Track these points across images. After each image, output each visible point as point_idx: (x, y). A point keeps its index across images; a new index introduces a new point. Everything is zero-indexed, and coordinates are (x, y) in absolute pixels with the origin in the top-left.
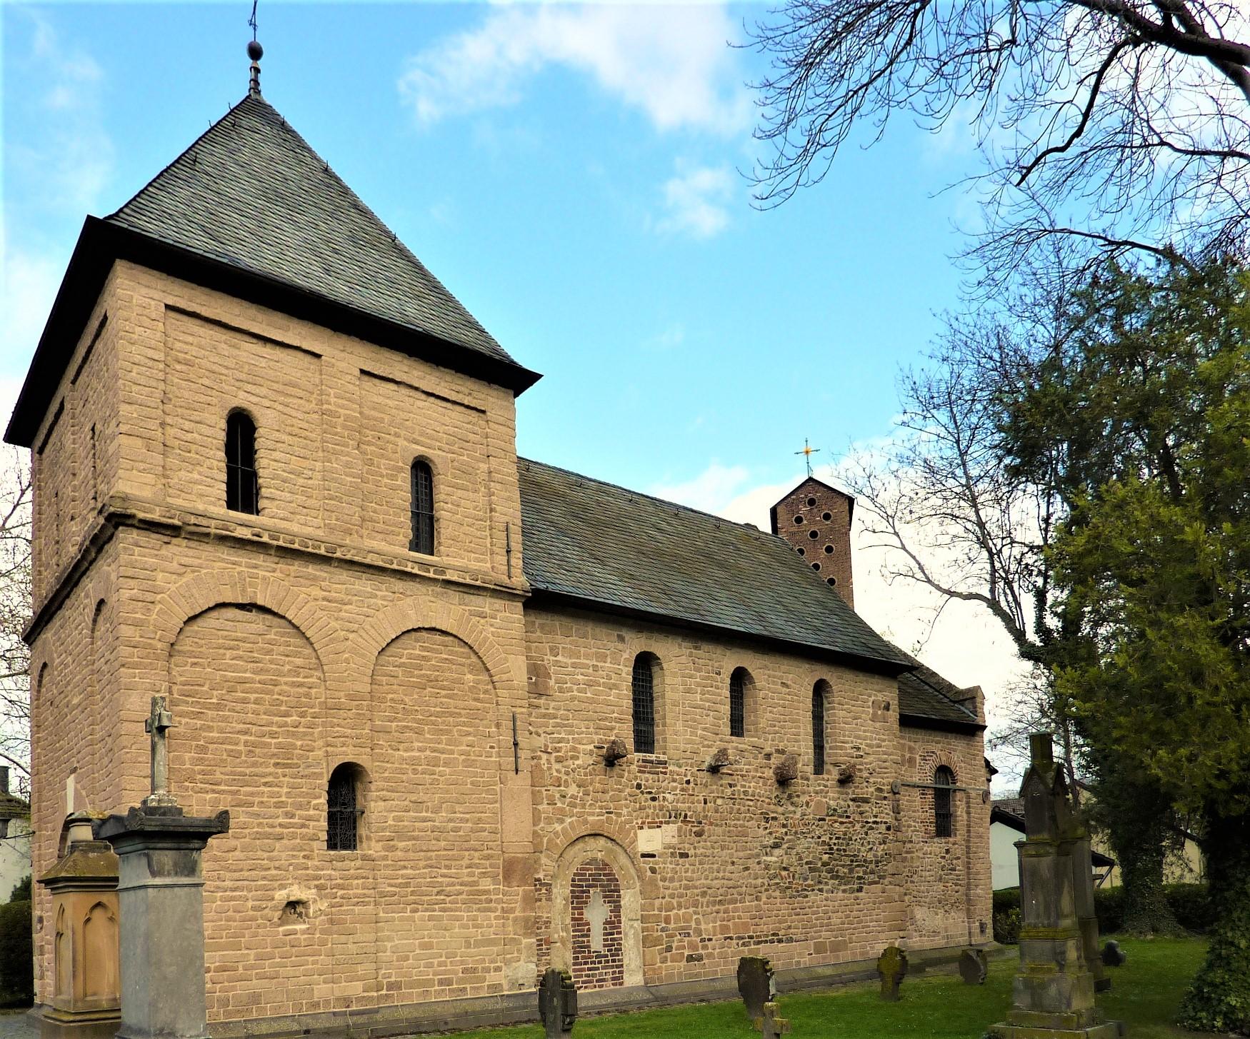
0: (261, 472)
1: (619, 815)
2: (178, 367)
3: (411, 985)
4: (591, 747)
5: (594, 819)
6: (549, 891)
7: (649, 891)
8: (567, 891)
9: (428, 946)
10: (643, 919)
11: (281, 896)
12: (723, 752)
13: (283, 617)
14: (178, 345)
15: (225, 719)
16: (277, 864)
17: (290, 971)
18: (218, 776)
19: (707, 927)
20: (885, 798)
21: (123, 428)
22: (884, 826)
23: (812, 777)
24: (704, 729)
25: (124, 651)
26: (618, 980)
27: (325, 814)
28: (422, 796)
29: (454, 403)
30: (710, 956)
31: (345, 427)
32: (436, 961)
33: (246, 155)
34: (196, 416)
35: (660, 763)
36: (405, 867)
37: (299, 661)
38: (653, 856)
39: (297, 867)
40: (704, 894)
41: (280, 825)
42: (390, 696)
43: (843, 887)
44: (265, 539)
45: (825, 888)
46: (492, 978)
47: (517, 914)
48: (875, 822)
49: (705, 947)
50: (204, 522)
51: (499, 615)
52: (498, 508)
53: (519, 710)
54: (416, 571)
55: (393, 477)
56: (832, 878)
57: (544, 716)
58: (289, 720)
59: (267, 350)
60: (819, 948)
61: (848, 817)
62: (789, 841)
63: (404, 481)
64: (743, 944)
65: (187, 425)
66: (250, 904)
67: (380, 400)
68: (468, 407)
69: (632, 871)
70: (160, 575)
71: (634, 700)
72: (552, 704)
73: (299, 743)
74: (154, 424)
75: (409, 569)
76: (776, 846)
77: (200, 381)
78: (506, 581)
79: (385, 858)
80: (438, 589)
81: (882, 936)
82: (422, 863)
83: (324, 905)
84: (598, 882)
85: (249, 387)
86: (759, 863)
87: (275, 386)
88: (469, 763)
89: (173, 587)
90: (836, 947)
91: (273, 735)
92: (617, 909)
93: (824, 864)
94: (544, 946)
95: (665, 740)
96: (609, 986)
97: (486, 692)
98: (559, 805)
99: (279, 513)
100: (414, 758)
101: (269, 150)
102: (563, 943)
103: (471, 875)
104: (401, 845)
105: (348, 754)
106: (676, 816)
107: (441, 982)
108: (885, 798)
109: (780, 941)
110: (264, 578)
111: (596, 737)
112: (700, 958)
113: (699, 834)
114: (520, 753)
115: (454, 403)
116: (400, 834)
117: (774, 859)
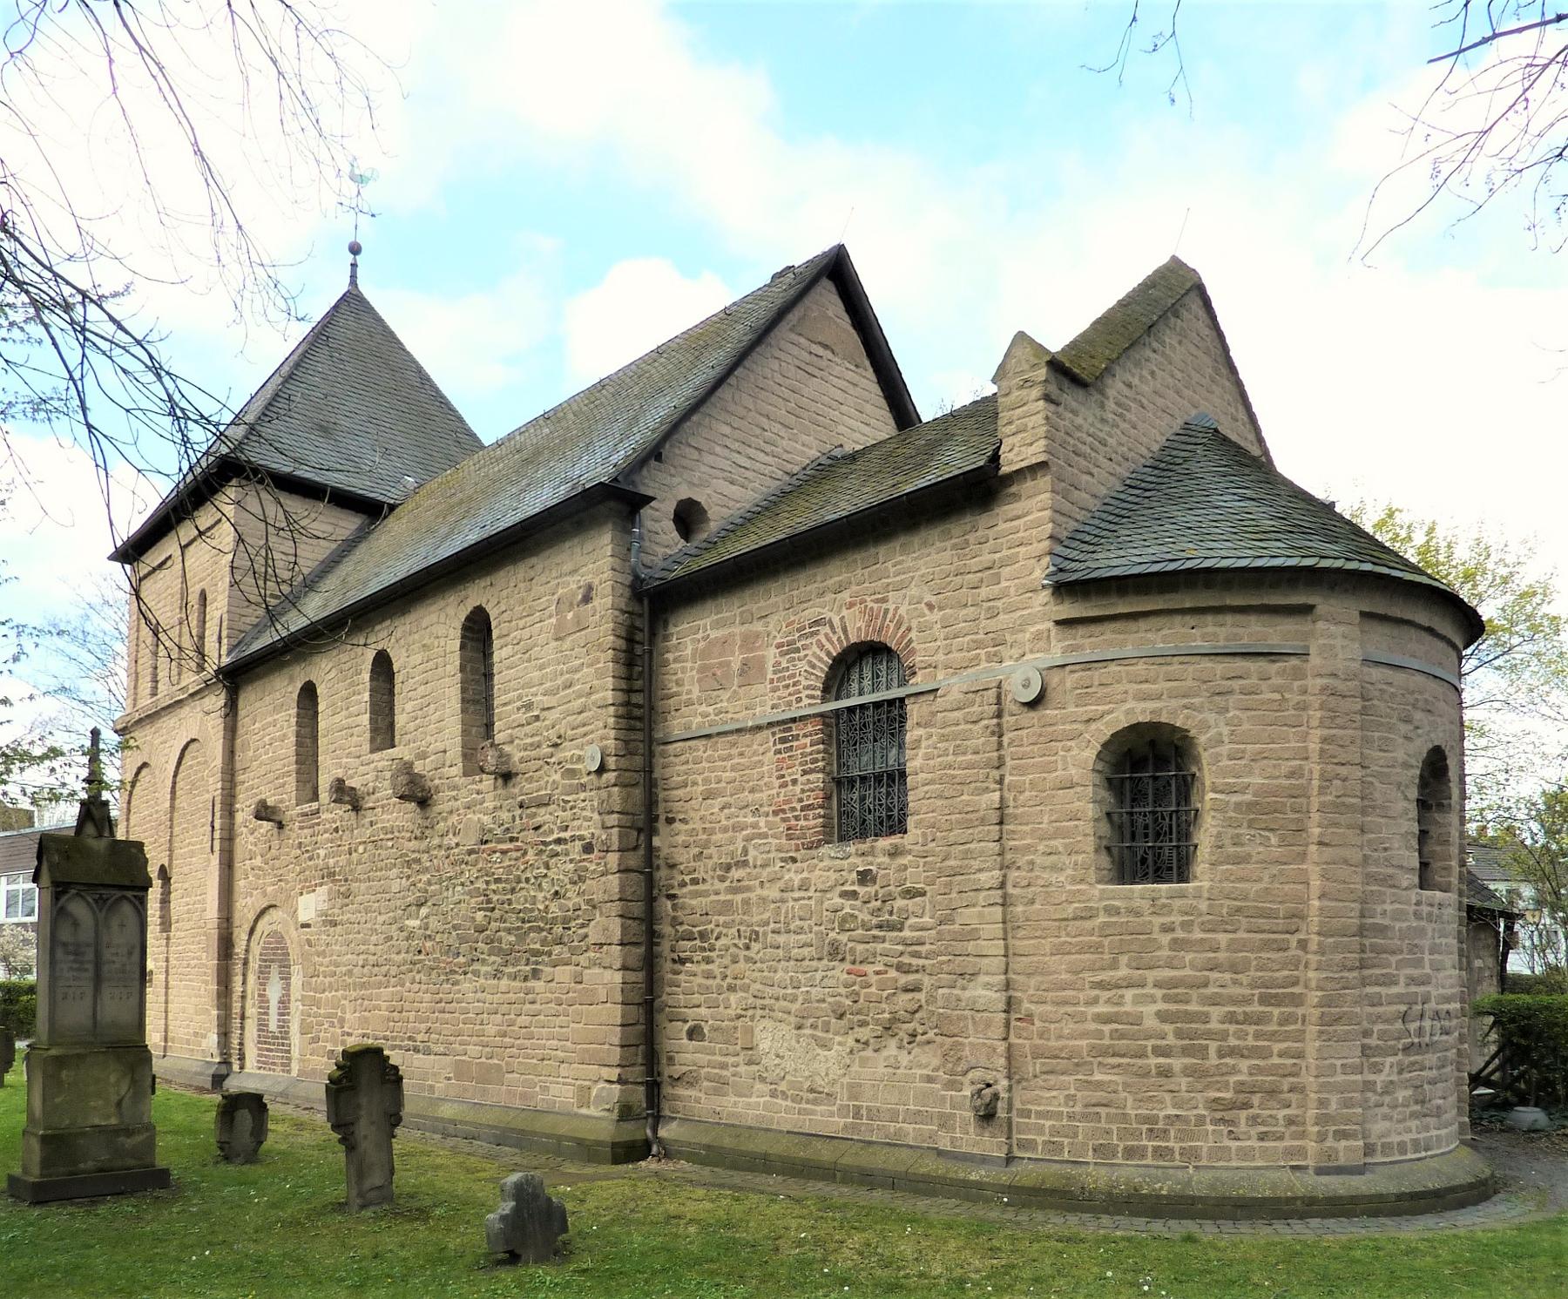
20: (583, 787)
22: (578, 844)
26: (286, 1066)
43: (510, 969)
45: (484, 969)
48: (559, 841)
60: (461, 1071)
61: (512, 840)
86: (401, 929)
90: (488, 1075)
108: (583, 787)
109: (416, 1050)
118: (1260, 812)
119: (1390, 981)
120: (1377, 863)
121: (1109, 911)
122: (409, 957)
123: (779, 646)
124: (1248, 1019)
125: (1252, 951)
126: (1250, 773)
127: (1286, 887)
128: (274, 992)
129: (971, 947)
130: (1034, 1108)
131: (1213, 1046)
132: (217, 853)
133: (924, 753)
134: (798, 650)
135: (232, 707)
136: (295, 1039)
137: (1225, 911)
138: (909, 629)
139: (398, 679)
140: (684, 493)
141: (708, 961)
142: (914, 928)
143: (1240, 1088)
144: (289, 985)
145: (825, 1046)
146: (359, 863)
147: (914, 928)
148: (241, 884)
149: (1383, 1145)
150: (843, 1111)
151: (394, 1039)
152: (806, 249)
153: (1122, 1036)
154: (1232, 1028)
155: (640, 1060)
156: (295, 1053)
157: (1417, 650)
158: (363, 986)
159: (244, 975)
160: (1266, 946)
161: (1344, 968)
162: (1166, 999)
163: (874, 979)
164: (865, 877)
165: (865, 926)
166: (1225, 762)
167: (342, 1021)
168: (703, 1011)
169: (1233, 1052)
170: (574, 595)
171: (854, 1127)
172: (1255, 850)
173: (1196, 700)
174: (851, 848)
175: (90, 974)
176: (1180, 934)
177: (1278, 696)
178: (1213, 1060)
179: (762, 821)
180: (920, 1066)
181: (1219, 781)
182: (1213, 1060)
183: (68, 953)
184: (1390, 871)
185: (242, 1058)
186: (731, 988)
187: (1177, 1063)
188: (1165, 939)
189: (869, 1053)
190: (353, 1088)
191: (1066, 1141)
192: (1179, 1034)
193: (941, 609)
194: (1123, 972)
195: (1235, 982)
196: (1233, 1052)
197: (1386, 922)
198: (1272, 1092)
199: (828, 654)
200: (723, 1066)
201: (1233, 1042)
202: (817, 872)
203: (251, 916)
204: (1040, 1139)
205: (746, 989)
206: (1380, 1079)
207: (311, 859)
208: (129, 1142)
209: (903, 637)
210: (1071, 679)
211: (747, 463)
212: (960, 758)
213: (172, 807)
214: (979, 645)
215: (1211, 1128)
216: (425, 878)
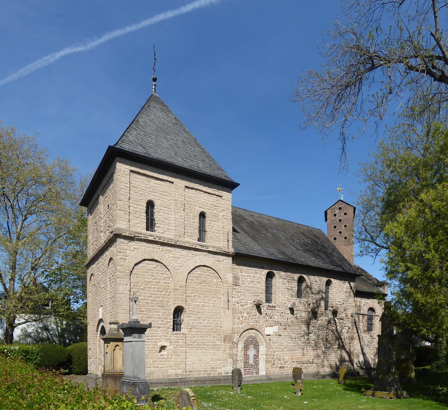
0: (156, 219)
1: (260, 323)
2: (133, 189)
3: (196, 371)
4: (252, 301)
5: (252, 324)
6: (237, 345)
7: (268, 347)
8: (243, 345)
9: (200, 360)
10: (266, 355)
11: (160, 344)
12: (294, 303)
13: (162, 263)
14: (133, 182)
15: (145, 293)
16: (158, 335)
17: (162, 366)
18: (143, 309)
19: (286, 358)
21: (118, 208)
24: (288, 296)
25: (118, 273)
26: (257, 373)
27: (172, 321)
28: (200, 316)
29: (213, 194)
30: (287, 367)
31: (180, 204)
32: (203, 365)
33: (152, 117)
34: (138, 203)
35: (273, 307)
36: (195, 337)
37: (166, 276)
38: (270, 335)
39: (164, 336)
40: (286, 348)
41: (160, 324)
42: (191, 286)
44: (157, 240)
46: (219, 370)
47: (228, 351)
49: (285, 364)
50: (140, 235)
51: (224, 261)
52: (225, 227)
53: (229, 290)
54: (200, 248)
55: (194, 219)
57: (237, 292)
58: (162, 293)
59: (158, 182)
62: (315, 332)
63: (197, 219)
64: (298, 364)
65: (136, 206)
66: (151, 346)
67: (191, 195)
68: (217, 195)
69: (263, 340)
70: (128, 251)
71: (266, 287)
72: (240, 288)
73: (165, 300)
74: (126, 206)
75: (198, 247)
77: (139, 192)
78: (227, 250)
79: (189, 334)
80: (207, 253)
82: (200, 336)
83: (171, 347)
84: (252, 343)
85: (153, 194)
87: (160, 193)
88: (214, 307)
89: (131, 254)
91: (158, 298)
92: (258, 351)
94: (235, 361)
95: (275, 299)
96: (255, 375)
97: (220, 285)
98: (241, 319)
99: (162, 231)
100: (198, 305)
101: (160, 114)
102: (241, 361)
103: (214, 340)
104: (194, 330)
105: (179, 304)
106: (277, 323)
107: (204, 371)
110: (156, 251)
111: (253, 298)
112: (284, 367)
114: (230, 304)
115: (213, 194)
116: (193, 327)
203: (242, 331)
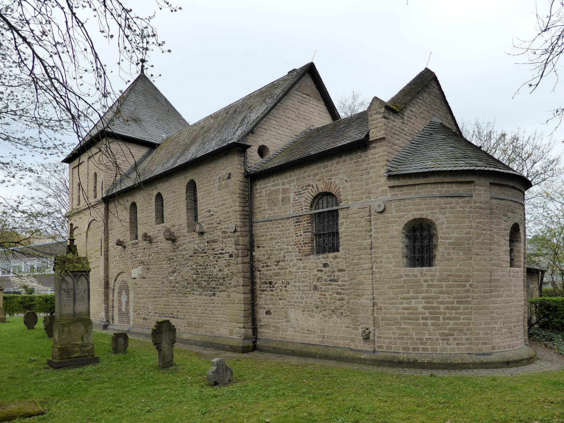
22: (227, 255)
23: (187, 234)
26: (128, 322)
30: (149, 319)
43: (205, 293)
45: (196, 293)
48: (221, 254)
56: (199, 287)
60: (189, 324)
61: (205, 253)
76: (174, 272)
81: (225, 324)
86: (167, 280)
90: (198, 326)
93: (195, 280)
109: (174, 317)
113: (148, 269)
117: (173, 278)
118: (457, 245)
119: (500, 296)
120: (495, 260)
121: (406, 276)
122: (170, 289)
123: (295, 193)
124: (453, 308)
125: (454, 288)
126: (453, 233)
127: (465, 268)
128: (124, 299)
129: (361, 287)
130: (382, 336)
131: (441, 317)
132: (103, 256)
133: (344, 226)
134: (301, 194)
135: (107, 209)
136: (131, 314)
137: (445, 276)
138: (339, 188)
139: (164, 202)
140: (261, 143)
141: (272, 291)
142: (342, 281)
143: (450, 329)
144: (129, 297)
145: (312, 317)
146: (153, 259)
147: (342, 281)
148: (111, 265)
149: (498, 346)
150: (319, 337)
151: (166, 314)
152: (300, 64)
153: (412, 314)
154: (448, 311)
155: (250, 321)
156: (132, 318)
157: (508, 194)
158: (155, 297)
159: (113, 294)
160: (459, 286)
161: (485, 292)
162: (426, 302)
163: (328, 296)
164: (325, 265)
165: (325, 280)
166: (445, 230)
167: (148, 308)
168: (271, 306)
169: (449, 318)
170: (225, 176)
171: (322, 341)
172: (454, 256)
173: (435, 211)
174: (321, 256)
175: (72, 298)
176: (430, 283)
177: (462, 209)
178: (441, 321)
179: (290, 247)
180: (344, 323)
181: (443, 236)
182: (441, 321)
183: (65, 292)
184: (500, 262)
185: (113, 320)
186: (280, 299)
187: (429, 322)
188: (425, 284)
189: (327, 319)
190: (160, 333)
191: (393, 346)
192: (430, 313)
193: (350, 182)
194: (411, 294)
195: (448, 297)
196: (449, 318)
197: (499, 278)
198: (461, 330)
199: (312, 195)
200: (278, 323)
201: (448, 315)
202: (309, 264)
203: (115, 276)
204: (384, 345)
205: (285, 299)
206: (497, 326)
207: (136, 258)
208: (86, 349)
209: (337, 190)
210: (393, 204)
211: (282, 133)
212: (357, 229)
213: (86, 241)
214: (363, 193)
215: (441, 342)
216: (175, 264)
